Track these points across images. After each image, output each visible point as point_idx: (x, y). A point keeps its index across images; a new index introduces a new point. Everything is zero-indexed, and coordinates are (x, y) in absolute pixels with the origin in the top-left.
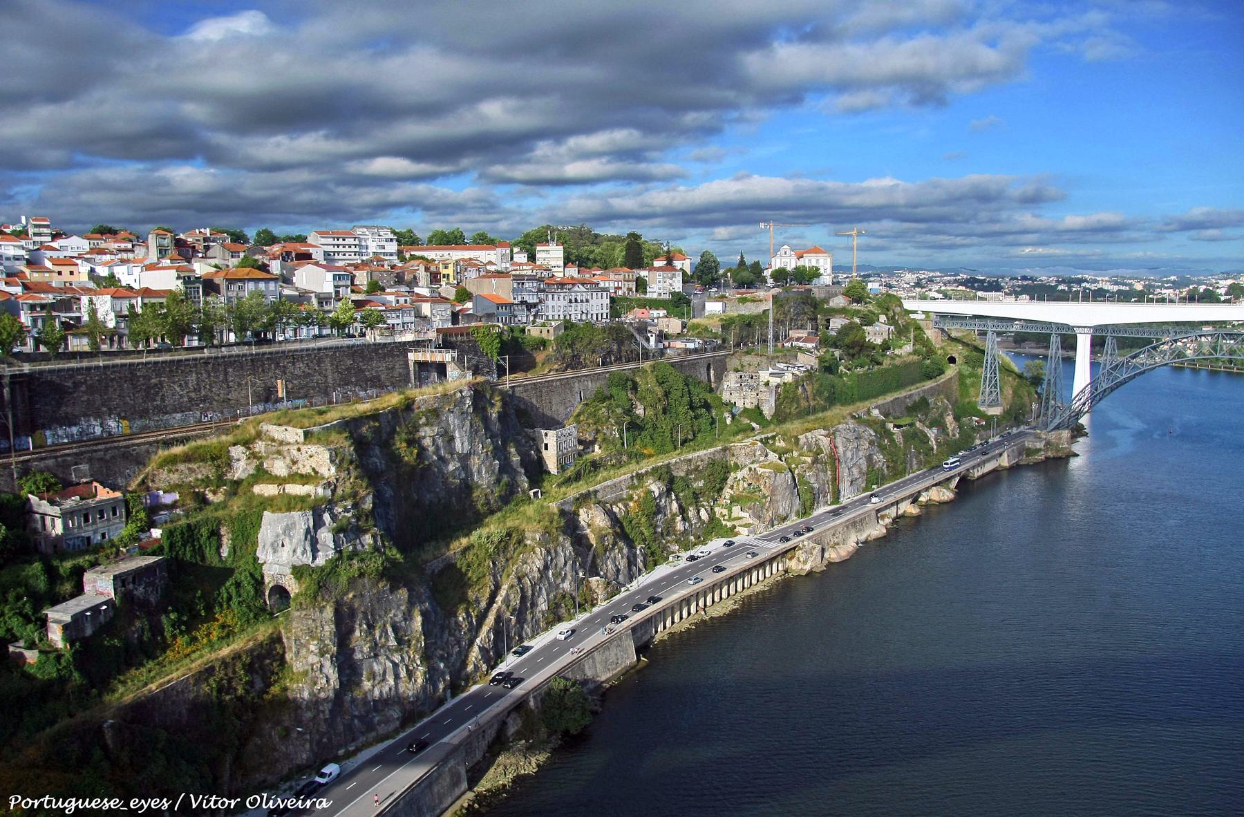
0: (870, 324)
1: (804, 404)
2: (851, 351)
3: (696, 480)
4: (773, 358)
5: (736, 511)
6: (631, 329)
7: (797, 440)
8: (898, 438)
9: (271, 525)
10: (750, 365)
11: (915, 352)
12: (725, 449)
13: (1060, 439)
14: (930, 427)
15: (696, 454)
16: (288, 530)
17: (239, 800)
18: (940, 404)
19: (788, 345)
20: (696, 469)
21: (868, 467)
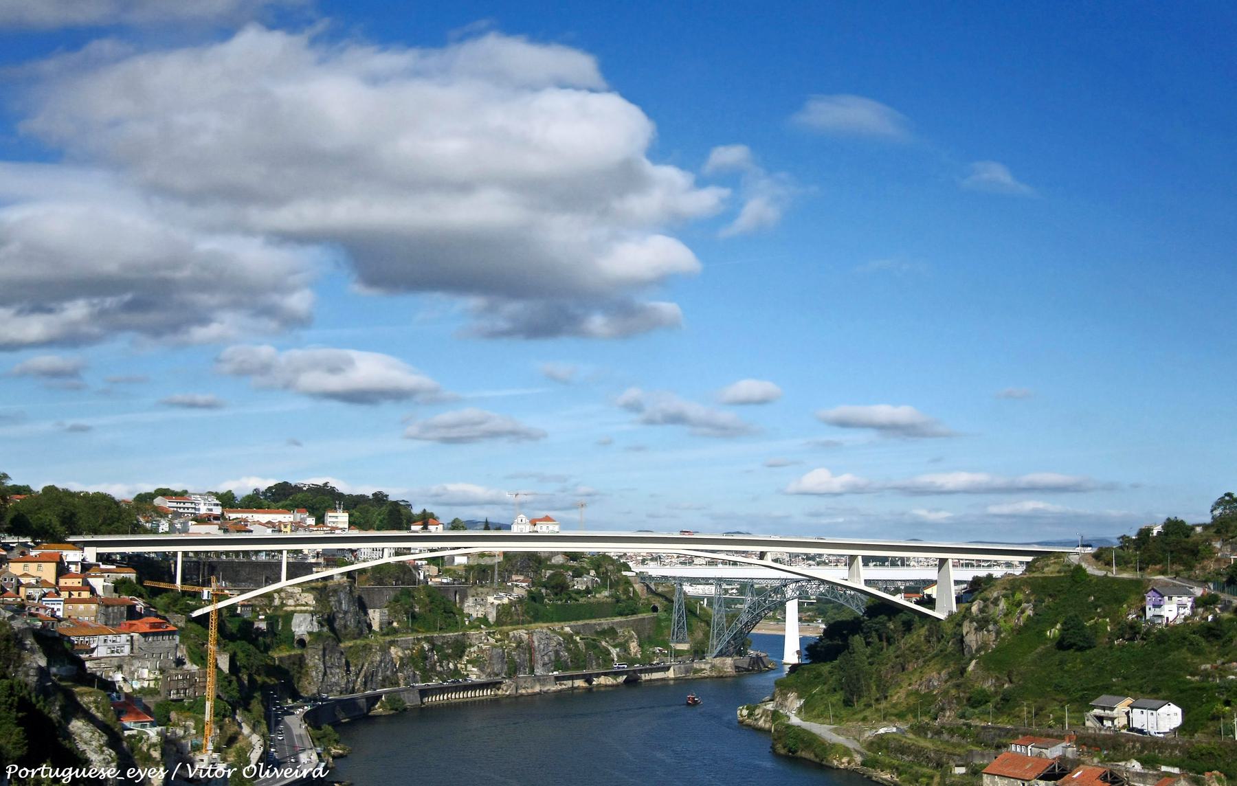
0: (580, 575)
1: (516, 618)
2: (555, 590)
3: (447, 649)
4: (497, 589)
5: (469, 667)
6: (410, 566)
7: (508, 635)
8: (582, 646)
9: (297, 619)
10: (482, 593)
11: (611, 596)
12: (464, 635)
13: (724, 664)
14: (615, 647)
15: (448, 634)
16: (305, 619)
17: (235, 769)
18: (626, 633)
19: (510, 584)
20: (447, 642)
21: (556, 657)
